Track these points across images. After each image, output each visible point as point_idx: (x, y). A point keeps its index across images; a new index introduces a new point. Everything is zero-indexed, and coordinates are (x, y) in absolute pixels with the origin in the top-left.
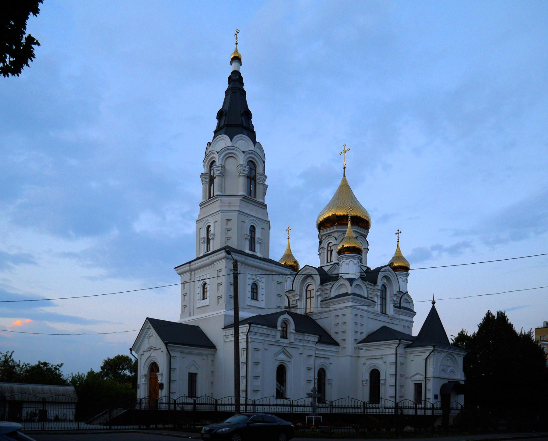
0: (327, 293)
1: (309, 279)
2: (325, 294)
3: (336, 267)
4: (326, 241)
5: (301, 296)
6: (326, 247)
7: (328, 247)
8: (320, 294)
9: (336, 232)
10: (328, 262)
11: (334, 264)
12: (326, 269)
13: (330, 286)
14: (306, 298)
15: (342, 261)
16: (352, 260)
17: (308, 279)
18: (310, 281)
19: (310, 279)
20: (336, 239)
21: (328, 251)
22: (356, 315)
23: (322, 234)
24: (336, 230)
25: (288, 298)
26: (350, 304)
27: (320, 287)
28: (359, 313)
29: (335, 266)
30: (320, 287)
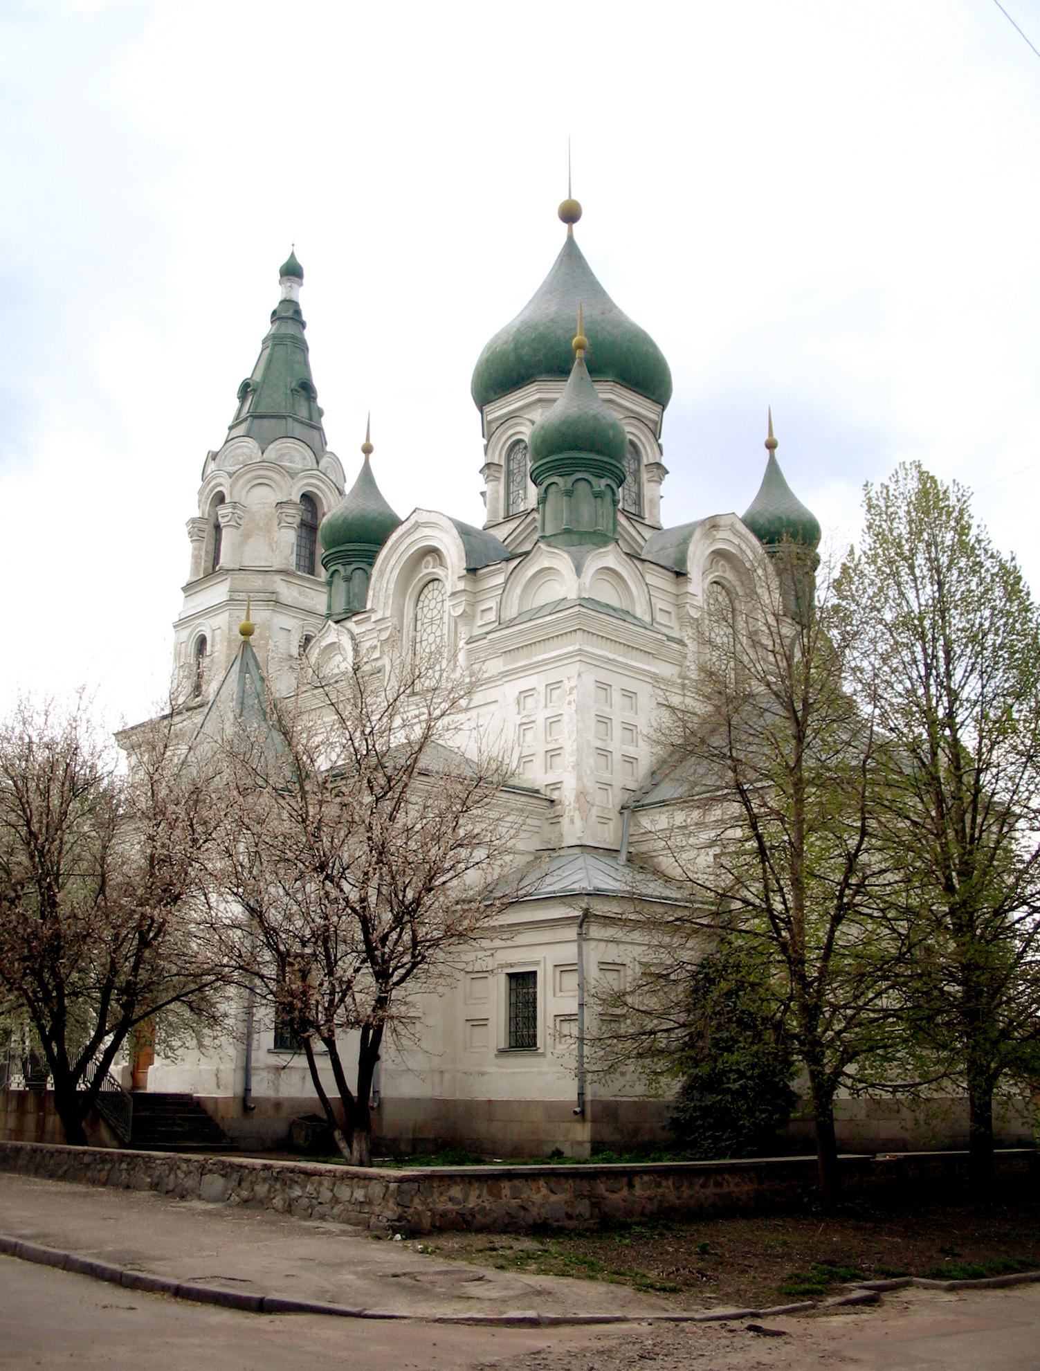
0: (491, 608)
2: (483, 611)
13: (500, 579)
23: (489, 418)
24: (537, 396)
27: (461, 585)
28: (618, 682)
29: (530, 524)
30: (461, 585)
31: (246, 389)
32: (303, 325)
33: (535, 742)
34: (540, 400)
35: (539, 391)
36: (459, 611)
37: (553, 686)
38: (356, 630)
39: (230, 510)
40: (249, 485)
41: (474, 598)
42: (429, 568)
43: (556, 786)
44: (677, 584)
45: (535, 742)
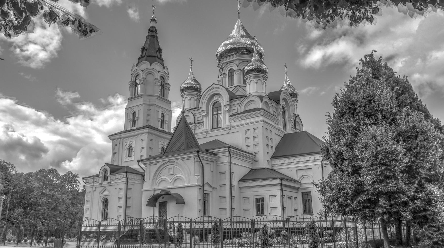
1: (216, 97)
2: (233, 110)
3: (238, 89)
4: (228, 67)
5: (207, 113)
6: (227, 73)
7: (229, 73)
8: (229, 110)
9: (237, 60)
10: (229, 86)
11: (237, 86)
12: (231, 90)
13: (238, 102)
14: (213, 115)
15: (250, 81)
16: (260, 79)
17: (215, 97)
18: (216, 98)
19: (217, 97)
20: (238, 66)
21: (229, 76)
22: (267, 129)
25: (194, 116)
26: (262, 118)
27: (228, 103)
29: (237, 89)
30: (228, 103)
31: (143, 49)
32: (157, 33)
33: (251, 142)
34: (238, 59)
35: (238, 57)
36: (227, 109)
37: (255, 129)
38: (194, 113)
39: (143, 80)
40: (147, 74)
41: (230, 106)
42: (215, 98)
43: (257, 153)
44: (277, 106)
45: (251, 142)
